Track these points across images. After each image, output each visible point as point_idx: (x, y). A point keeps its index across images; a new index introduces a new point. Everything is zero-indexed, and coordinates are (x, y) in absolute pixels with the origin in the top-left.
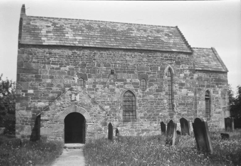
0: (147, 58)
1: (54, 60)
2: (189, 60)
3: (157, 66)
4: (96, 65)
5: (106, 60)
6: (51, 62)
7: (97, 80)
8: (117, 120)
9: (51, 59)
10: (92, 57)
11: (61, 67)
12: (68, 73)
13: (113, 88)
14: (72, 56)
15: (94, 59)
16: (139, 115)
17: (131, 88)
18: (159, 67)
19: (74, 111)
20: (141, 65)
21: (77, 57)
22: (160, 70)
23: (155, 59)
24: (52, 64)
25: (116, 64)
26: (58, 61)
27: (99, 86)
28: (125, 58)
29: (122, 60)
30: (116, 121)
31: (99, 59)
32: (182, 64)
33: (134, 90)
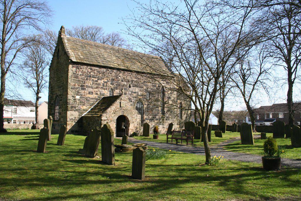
1: (94, 74)
9: (92, 73)
10: (118, 74)
12: (103, 85)
14: (105, 73)
15: (120, 76)
19: (122, 114)
22: (158, 87)
24: (92, 77)
26: (97, 76)
31: (122, 77)
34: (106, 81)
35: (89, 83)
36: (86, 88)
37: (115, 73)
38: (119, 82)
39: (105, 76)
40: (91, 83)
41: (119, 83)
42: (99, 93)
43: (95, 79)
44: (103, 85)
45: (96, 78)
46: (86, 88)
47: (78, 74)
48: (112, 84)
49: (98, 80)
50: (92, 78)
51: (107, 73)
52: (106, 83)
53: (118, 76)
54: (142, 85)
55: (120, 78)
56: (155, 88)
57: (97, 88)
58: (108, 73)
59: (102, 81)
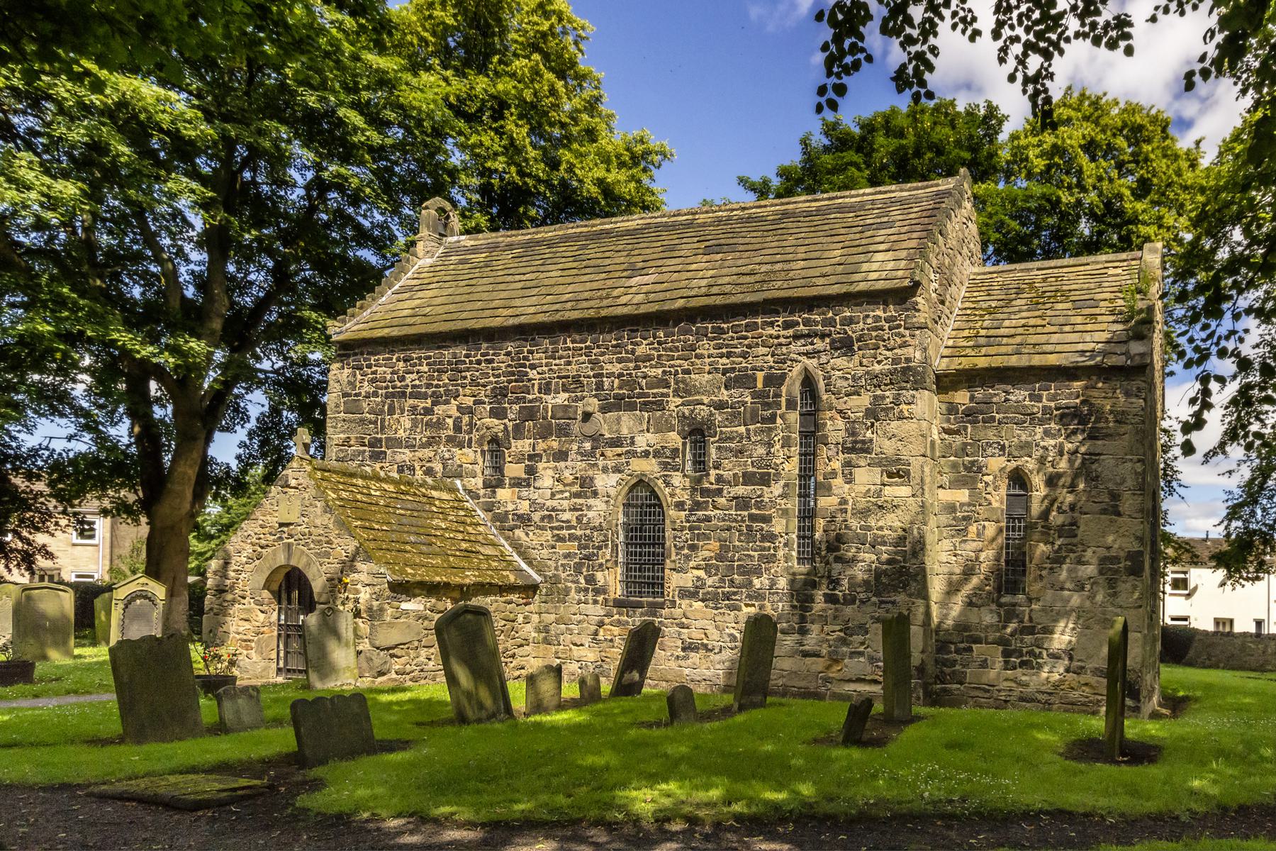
0: (714, 338)
1: (417, 382)
2: (899, 326)
3: (754, 369)
4: (536, 387)
5: (569, 363)
6: (409, 390)
7: (541, 445)
8: (600, 598)
9: (409, 377)
10: (525, 358)
11: (434, 404)
13: (590, 473)
15: (533, 367)
16: (675, 581)
17: (649, 467)
18: (760, 376)
20: (687, 372)
21: (479, 362)
23: (746, 338)
24: (412, 396)
25: (601, 375)
27: (545, 469)
28: (633, 352)
29: (620, 361)
30: (595, 602)
32: (860, 349)
33: (660, 482)
34: (469, 401)
35: (402, 425)
36: (389, 452)
37: (508, 354)
38: (531, 397)
39: (465, 378)
40: (408, 425)
41: (530, 401)
42: (438, 467)
43: (422, 404)
44: (458, 428)
45: (425, 396)
46: (389, 452)
47: (359, 394)
48: (495, 414)
49: (434, 404)
50: (411, 401)
51: (471, 362)
52: (470, 411)
53: (524, 366)
54: (655, 395)
55: (533, 374)
56: (749, 399)
57: (428, 444)
58: (479, 362)
59: (452, 409)
